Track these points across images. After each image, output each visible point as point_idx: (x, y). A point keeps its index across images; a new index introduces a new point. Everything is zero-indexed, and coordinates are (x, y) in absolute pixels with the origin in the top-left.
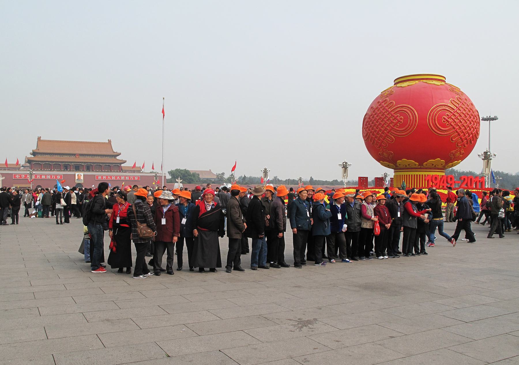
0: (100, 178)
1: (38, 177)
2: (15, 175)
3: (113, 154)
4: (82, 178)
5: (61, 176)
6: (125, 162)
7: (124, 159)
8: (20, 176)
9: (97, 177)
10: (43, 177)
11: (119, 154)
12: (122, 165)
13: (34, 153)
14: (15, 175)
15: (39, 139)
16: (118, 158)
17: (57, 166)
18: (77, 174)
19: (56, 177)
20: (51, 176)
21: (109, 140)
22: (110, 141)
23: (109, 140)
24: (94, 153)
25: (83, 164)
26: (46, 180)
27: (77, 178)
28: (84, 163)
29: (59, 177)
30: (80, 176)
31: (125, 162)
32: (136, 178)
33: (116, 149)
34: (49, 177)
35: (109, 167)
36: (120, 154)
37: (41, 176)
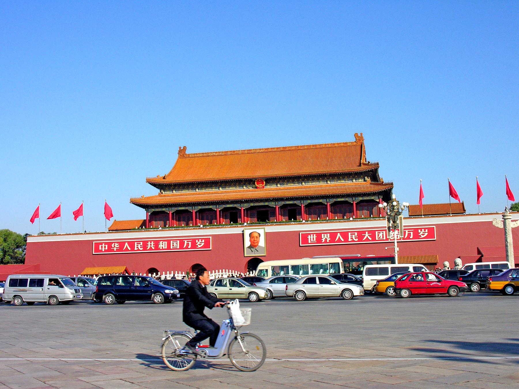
0: (312, 239)
1: (151, 245)
2: (97, 245)
3: (355, 168)
4: (262, 243)
5: (207, 242)
8: (109, 244)
9: (305, 238)
10: (161, 246)
14: (97, 245)
15: (182, 152)
17: (207, 214)
18: (247, 233)
19: (194, 245)
20: (182, 243)
21: (356, 135)
23: (356, 135)
25: (272, 204)
26: (169, 252)
27: (247, 243)
29: (200, 244)
32: (423, 234)
35: (342, 206)
37: (157, 243)
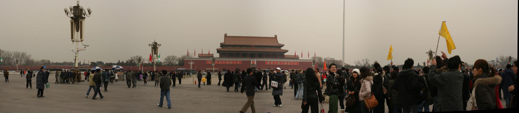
0: (268, 63)
4: (255, 63)
6: (287, 51)
7: (286, 49)
11: (283, 45)
12: (285, 54)
13: (222, 45)
15: (226, 35)
16: (282, 48)
18: (252, 60)
22: (276, 36)
24: (264, 44)
26: (229, 65)
28: (257, 52)
30: (254, 61)
31: (287, 51)
33: (280, 41)
34: (231, 63)
36: (283, 45)
37: (226, 62)
